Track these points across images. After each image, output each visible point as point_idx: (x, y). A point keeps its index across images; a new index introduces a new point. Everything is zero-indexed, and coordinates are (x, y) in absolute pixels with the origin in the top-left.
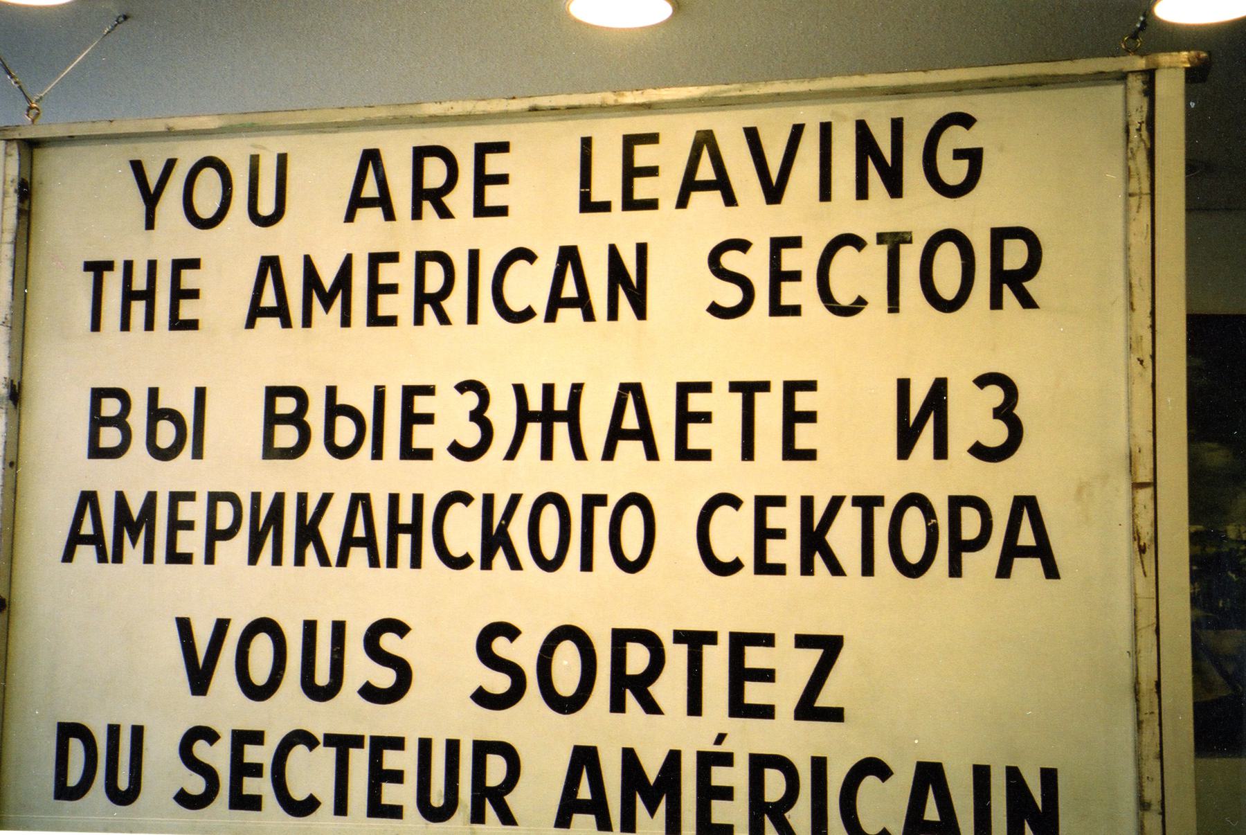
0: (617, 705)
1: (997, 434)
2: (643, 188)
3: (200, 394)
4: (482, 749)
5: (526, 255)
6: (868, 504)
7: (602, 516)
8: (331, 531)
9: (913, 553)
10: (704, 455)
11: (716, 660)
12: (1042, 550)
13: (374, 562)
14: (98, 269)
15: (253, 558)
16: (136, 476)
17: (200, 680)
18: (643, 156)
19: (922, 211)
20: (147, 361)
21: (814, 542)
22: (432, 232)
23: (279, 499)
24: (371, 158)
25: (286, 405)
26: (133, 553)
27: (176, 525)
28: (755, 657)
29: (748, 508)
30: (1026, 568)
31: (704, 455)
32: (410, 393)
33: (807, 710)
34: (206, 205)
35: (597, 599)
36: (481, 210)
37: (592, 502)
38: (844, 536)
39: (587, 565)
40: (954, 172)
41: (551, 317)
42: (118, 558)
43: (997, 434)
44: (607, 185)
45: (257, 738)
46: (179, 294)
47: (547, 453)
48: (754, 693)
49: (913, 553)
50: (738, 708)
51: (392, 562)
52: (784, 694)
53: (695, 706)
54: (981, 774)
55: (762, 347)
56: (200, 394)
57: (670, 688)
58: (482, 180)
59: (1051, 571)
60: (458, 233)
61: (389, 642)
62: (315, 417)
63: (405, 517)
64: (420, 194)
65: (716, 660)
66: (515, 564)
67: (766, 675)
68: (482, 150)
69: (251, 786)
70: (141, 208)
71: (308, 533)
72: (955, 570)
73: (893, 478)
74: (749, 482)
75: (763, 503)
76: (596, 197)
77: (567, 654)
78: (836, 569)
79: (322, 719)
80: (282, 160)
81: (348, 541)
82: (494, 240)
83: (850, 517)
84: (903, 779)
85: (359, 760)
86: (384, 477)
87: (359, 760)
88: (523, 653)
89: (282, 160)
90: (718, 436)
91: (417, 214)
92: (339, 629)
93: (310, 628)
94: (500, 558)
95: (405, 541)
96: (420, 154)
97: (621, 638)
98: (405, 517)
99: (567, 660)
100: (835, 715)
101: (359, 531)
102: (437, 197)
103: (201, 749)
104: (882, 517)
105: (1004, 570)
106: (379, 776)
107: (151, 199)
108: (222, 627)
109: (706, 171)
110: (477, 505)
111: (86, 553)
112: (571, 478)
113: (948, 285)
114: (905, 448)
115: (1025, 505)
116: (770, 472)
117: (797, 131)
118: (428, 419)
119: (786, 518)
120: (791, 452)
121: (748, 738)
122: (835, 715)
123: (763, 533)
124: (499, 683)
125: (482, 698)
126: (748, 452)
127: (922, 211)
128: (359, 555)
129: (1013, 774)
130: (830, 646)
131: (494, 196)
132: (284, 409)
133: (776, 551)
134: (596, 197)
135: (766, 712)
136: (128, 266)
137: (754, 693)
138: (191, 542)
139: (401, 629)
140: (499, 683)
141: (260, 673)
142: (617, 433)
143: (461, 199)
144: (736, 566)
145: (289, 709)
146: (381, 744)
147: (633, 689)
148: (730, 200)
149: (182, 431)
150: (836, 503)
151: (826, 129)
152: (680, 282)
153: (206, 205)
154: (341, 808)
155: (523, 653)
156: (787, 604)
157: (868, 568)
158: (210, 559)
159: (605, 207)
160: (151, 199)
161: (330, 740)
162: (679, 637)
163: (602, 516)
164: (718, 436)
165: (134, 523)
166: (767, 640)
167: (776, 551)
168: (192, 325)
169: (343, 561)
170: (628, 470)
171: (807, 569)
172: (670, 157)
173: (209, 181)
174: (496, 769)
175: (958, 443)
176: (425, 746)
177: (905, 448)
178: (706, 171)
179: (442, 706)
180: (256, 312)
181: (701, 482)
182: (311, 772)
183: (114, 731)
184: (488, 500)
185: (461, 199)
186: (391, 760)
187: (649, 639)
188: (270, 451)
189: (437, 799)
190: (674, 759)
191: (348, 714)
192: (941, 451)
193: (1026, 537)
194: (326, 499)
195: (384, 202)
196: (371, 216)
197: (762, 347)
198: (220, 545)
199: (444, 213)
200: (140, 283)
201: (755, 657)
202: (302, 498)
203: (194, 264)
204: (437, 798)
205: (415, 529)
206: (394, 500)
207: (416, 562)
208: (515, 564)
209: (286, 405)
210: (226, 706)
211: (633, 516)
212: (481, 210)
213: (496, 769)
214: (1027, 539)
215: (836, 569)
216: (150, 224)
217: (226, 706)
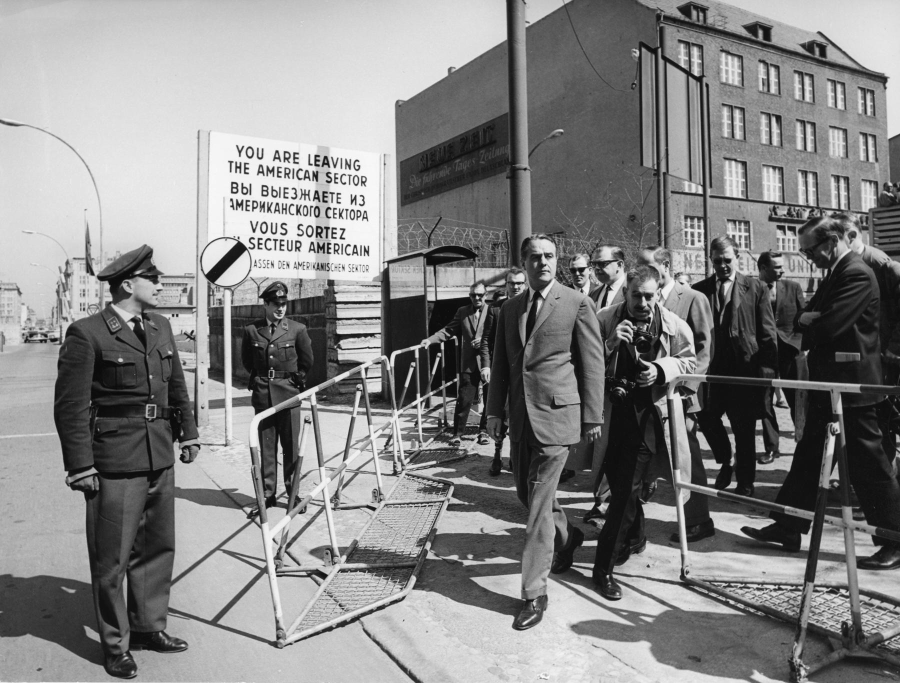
4: (297, 242)
8: (273, 208)
11: (330, 232)
14: (231, 162)
16: (240, 197)
17: (254, 231)
20: (240, 178)
21: (340, 215)
25: (265, 188)
38: (344, 215)
44: (312, 162)
46: (245, 168)
57: (324, 235)
58: (295, 158)
60: (291, 165)
62: (270, 191)
64: (285, 159)
68: (295, 154)
71: (269, 209)
73: (350, 207)
75: (335, 209)
77: (310, 229)
79: (273, 237)
82: (296, 167)
83: (345, 212)
85: (278, 243)
86: (281, 200)
96: (285, 152)
102: (287, 159)
107: (240, 152)
113: (356, 182)
119: (337, 211)
121: (333, 242)
123: (334, 214)
124: (301, 233)
127: (353, 172)
130: (344, 230)
132: (265, 190)
138: (250, 208)
141: (264, 230)
142: (315, 198)
143: (291, 160)
145: (268, 235)
146: (281, 241)
155: (304, 228)
160: (240, 152)
163: (313, 209)
165: (240, 204)
174: (298, 245)
179: (292, 235)
181: (326, 205)
182: (270, 244)
185: (291, 160)
187: (321, 228)
191: (278, 236)
212: (295, 163)
217: (258, 234)
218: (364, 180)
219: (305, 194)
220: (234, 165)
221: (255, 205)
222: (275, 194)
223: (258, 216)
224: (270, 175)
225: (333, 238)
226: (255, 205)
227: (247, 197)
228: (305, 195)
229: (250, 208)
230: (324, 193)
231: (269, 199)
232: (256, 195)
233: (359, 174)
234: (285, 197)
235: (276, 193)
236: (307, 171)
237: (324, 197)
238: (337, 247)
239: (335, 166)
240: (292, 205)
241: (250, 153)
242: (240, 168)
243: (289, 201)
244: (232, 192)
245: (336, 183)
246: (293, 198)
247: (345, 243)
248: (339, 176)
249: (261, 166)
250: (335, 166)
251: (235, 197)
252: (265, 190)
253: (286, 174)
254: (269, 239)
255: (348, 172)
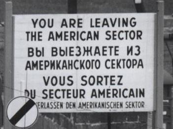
0: (98, 84)
1: (137, 52)
2: (98, 25)
3: (43, 48)
4: (81, 90)
5: (84, 32)
6: (124, 60)
7: (94, 62)
8: (61, 65)
9: (129, 65)
10: (106, 55)
11: (109, 79)
12: (142, 65)
13: (66, 69)
14: (28, 33)
15: (51, 68)
16: (35, 59)
17: (46, 84)
18: (98, 21)
19: (129, 28)
20: (35, 44)
21: (118, 64)
22: (72, 29)
23: (54, 61)
24: (64, 20)
26: (35, 69)
27: (41, 65)
28: (113, 78)
29: (111, 61)
30: (140, 67)
31: (106, 55)
32: (70, 48)
33: (119, 84)
34: (42, 25)
35: (94, 72)
36: (79, 27)
37: (93, 61)
38: (121, 64)
39: (92, 68)
40: (133, 24)
41: (87, 39)
42: (33, 69)
43: (137, 52)
44: (94, 24)
45: (52, 90)
46: (39, 36)
47: (88, 55)
48: (113, 82)
49: (129, 65)
50: (111, 84)
51: (69, 68)
52: (116, 82)
53: (106, 84)
54: (137, 90)
55: (112, 43)
56: (43, 48)
57: (104, 82)
58: (79, 23)
59: (143, 67)
61: (70, 79)
62: (58, 51)
63: (70, 63)
64: (71, 24)
65: (109, 79)
66: (84, 68)
67: (114, 80)
68: (79, 20)
69: (52, 96)
70: (33, 25)
71: (58, 66)
72: (133, 67)
73: (127, 58)
74: (111, 58)
75: (113, 60)
76: (93, 25)
77: (92, 79)
78: (120, 67)
79: (61, 88)
80: (53, 20)
81: (63, 66)
82: (80, 30)
83: (122, 62)
84: (129, 91)
85: (66, 92)
86: (67, 58)
87: (66, 92)
88: (87, 79)
89: (53, 20)
90: (108, 53)
91: (70, 27)
92: (64, 77)
93: (60, 77)
94: (82, 68)
95: (70, 66)
96: (71, 20)
97: (98, 77)
98: (70, 63)
99: (92, 79)
100: (122, 84)
101: (65, 65)
102: (73, 25)
103: (45, 92)
104: (125, 62)
105: (138, 67)
106: (68, 94)
108: (49, 77)
109: (105, 23)
110: (79, 62)
111: (28, 69)
112: (90, 58)
113: (132, 36)
114: (128, 54)
115: (141, 60)
116: (113, 57)
117: (116, 19)
118: (73, 51)
119: (115, 62)
120: (116, 54)
121: (112, 87)
122: (122, 84)
123: (113, 64)
124: (84, 83)
125: (82, 85)
126: (111, 54)
127: (129, 28)
128: (65, 68)
129: (140, 90)
130: (121, 77)
131: (80, 25)
132: (54, 51)
133: (114, 66)
134: (93, 25)
135: (114, 84)
136: (32, 33)
137: (113, 82)
138: (43, 67)
139: (71, 77)
140: (84, 83)
143: (76, 25)
144: (109, 68)
145: (58, 86)
146: (68, 90)
147: (99, 83)
148: (108, 26)
149: (41, 53)
150: (120, 60)
151: (119, 19)
152: (103, 35)
153: (42, 25)
154: (64, 97)
155: (87, 79)
156: (116, 72)
157: (124, 67)
158: (45, 69)
159: (93, 27)
161: (62, 90)
162: (105, 76)
163: (94, 62)
164: (108, 53)
165: (35, 65)
166: (114, 76)
167: (114, 66)
168: (41, 40)
169: (63, 69)
170: (97, 57)
171: (117, 68)
172: (101, 21)
173: (43, 22)
174: (82, 92)
175: (134, 53)
176: (74, 90)
177: (128, 54)
178: (105, 23)
179: (77, 85)
180: (50, 38)
181: (105, 58)
182: (59, 94)
183: (31, 91)
184: (81, 61)
185: (76, 25)
186: (69, 92)
188: (53, 55)
189: (75, 95)
190: (104, 90)
191: (66, 87)
192: (132, 54)
193: (140, 64)
194: (60, 61)
195: (66, 25)
196: (64, 27)
197: (112, 43)
198: (47, 68)
199: (74, 27)
200: (34, 34)
201: (113, 78)
202: (57, 61)
203: (41, 32)
204: (75, 95)
205: (72, 65)
206: (69, 61)
207: (72, 68)
208: (84, 68)
209: (54, 50)
210: (50, 86)
211: (98, 63)
212: (79, 27)
213: (82, 92)
214: (141, 64)
215: (120, 67)
216: (35, 27)
218: (139, 33)
219: (88, 51)
220: (30, 35)
221: (47, 64)
222: (62, 53)
223: (49, 72)
224: (59, 40)
225: (111, 84)
226: (47, 64)
227: (41, 58)
228: (88, 51)
229: (43, 67)
230: (104, 47)
231: (58, 58)
232: (48, 56)
233: (135, 29)
234: (70, 55)
235: (63, 52)
236: (89, 33)
237: (104, 51)
238: (115, 92)
239: (113, 25)
240: (77, 61)
241: (42, 23)
242: (35, 36)
243: (74, 58)
244: (29, 56)
245: (114, 39)
246: (77, 55)
247: (122, 88)
248: (117, 34)
249: (51, 33)
250: (113, 25)
251: (31, 59)
252: (54, 51)
253: (71, 36)
254: (59, 90)
255: (125, 29)
